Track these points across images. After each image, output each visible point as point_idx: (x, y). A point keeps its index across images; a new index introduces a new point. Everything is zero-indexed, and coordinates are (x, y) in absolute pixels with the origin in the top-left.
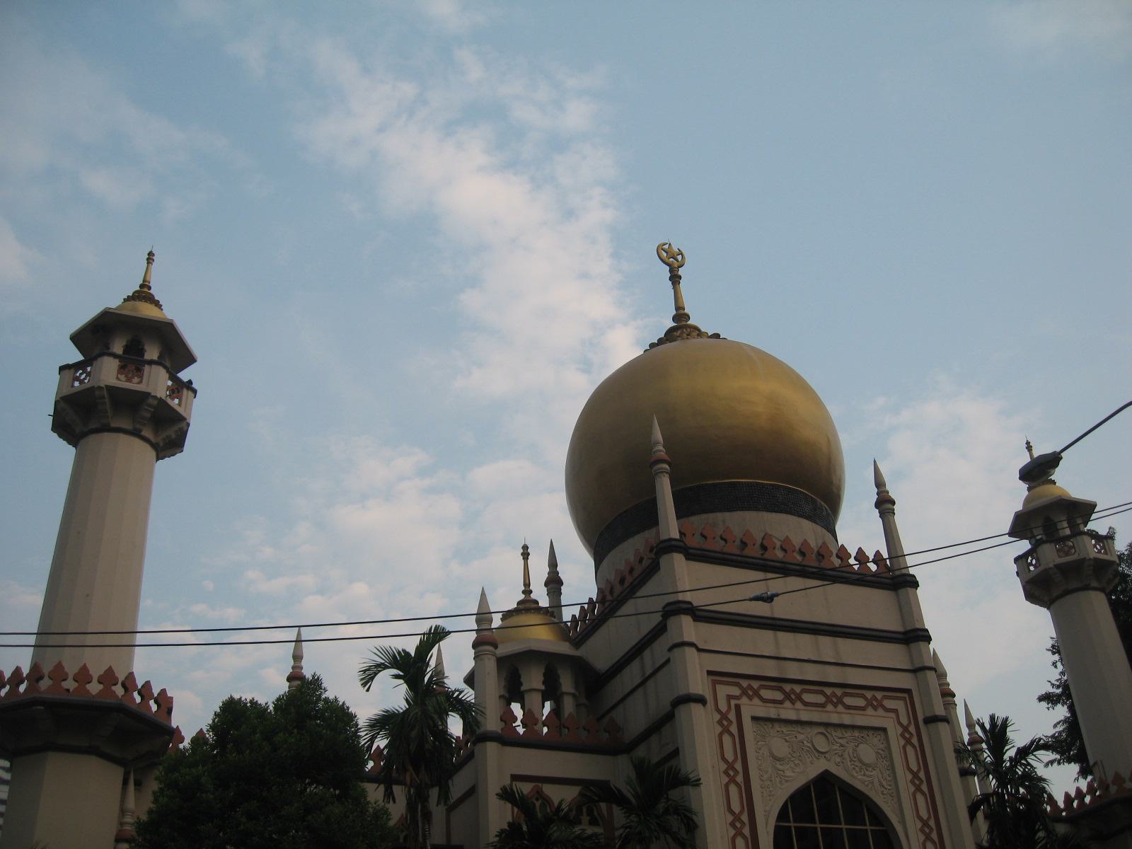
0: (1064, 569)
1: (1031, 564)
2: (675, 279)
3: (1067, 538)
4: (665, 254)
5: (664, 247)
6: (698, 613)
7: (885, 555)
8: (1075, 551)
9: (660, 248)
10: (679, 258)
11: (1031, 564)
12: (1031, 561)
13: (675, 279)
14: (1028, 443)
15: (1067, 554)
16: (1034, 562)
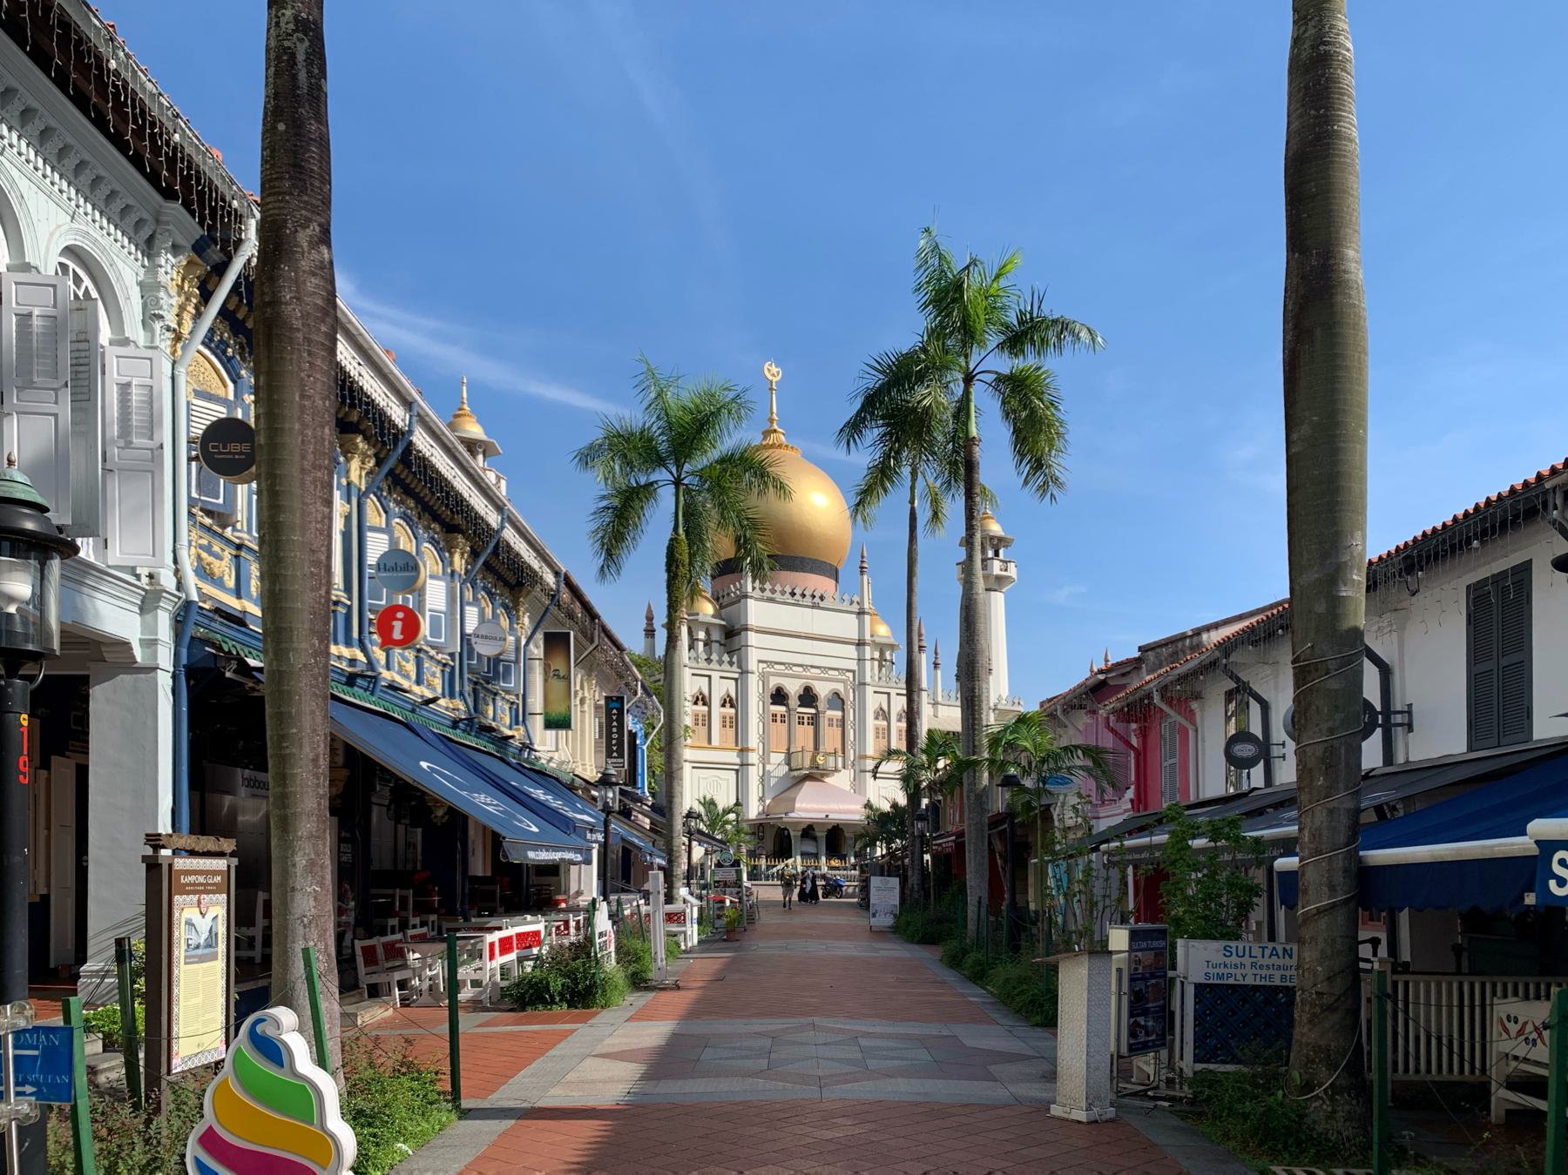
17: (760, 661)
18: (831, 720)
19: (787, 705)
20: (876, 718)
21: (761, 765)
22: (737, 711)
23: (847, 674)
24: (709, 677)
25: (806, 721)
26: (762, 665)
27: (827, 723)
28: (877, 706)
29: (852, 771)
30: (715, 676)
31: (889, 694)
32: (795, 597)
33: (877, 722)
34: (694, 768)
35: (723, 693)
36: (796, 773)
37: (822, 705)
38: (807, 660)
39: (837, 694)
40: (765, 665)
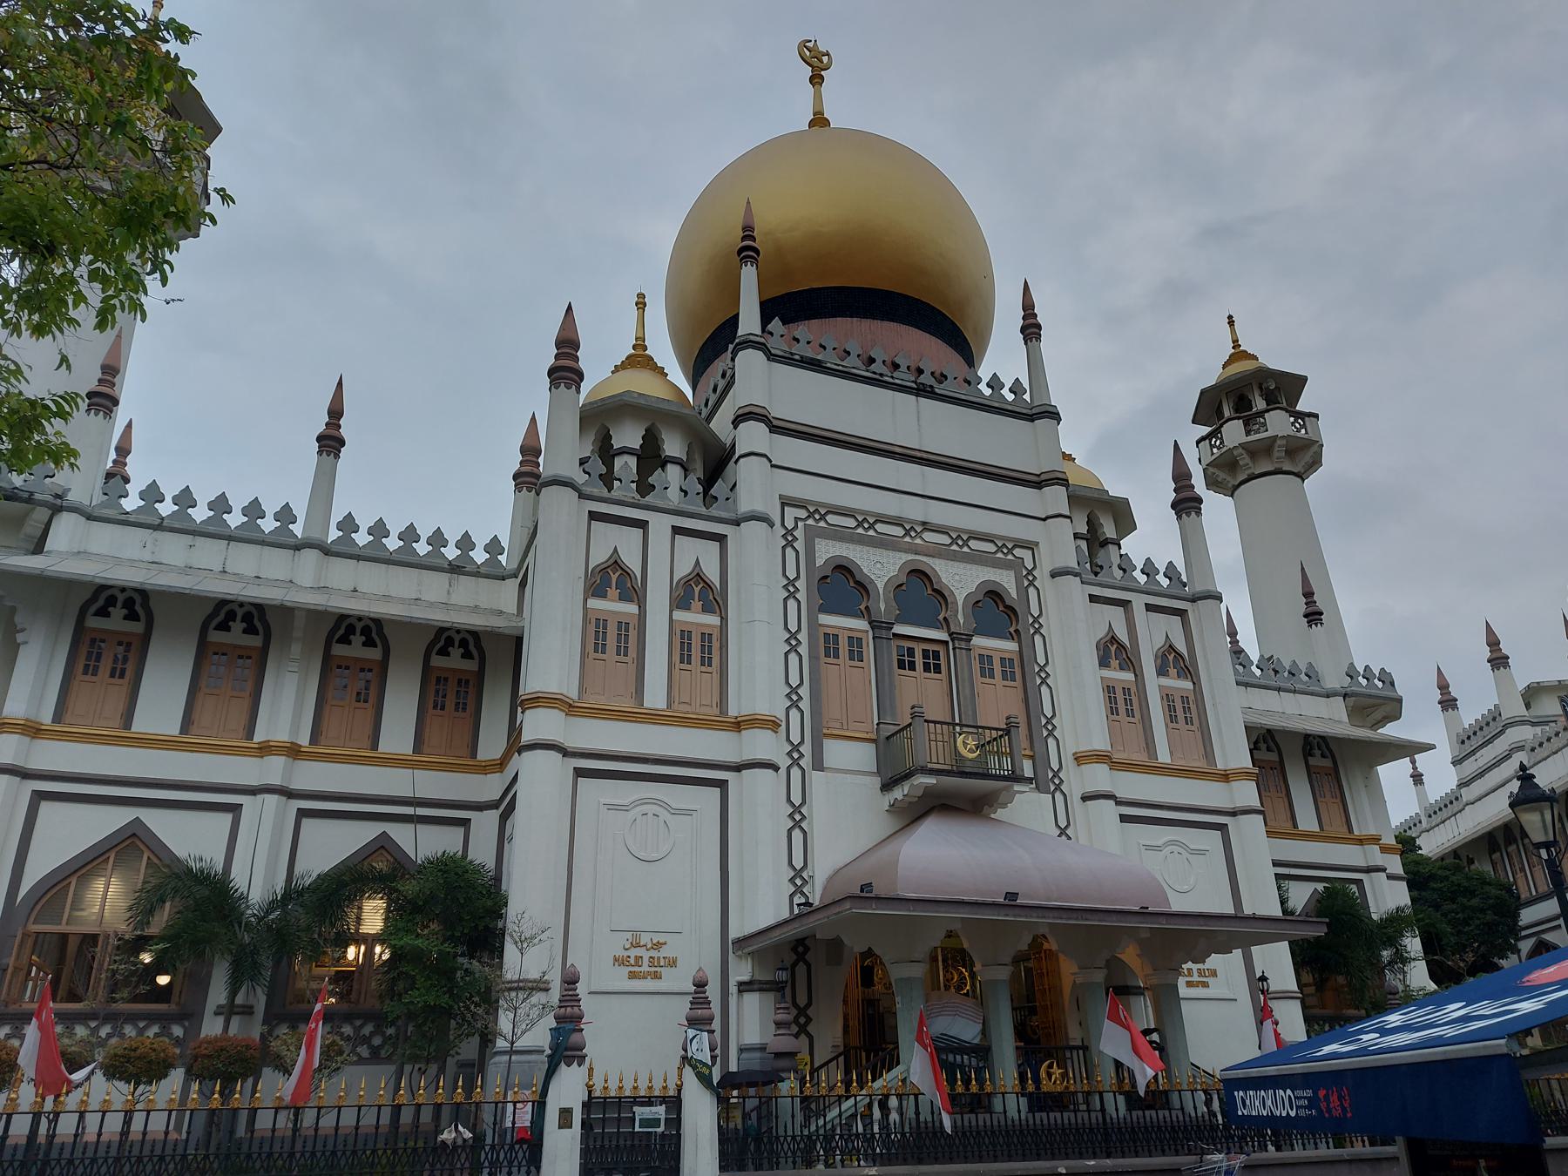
0: (1254, 451)
1: (1215, 446)
2: (816, 79)
3: (1261, 414)
4: (808, 53)
5: (807, 44)
6: (775, 423)
7: (1026, 385)
8: (1267, 430)
9: (804, 44)
10: (825, 59)
11: (1215, 446)
12: (1215, 442)
13: (816, 79)
14: (1230, 317)
15: (1257, 432)
16: (1218, 443)
17: (786, 502)
18: (986, 660)
19: (866, 614)
20: (1104, 663)
21: (795, 772)
22: (724, 619)
23: (1018, 552)
24: (642, 525)
25: (919, 660)
26: (790, 513)
27: (976, 666)
28: (1101, 632)
29: (1058, 795)
30: (661, 525)
31: (1124, 604)
32: (873, 367)
33: (1107, 673)
34: (580, 773)
35: (684, 569)
36: (898, 793)
37: (961, 620)
38: (914, 510)
39: (993, 594)
40: (803, 514)
